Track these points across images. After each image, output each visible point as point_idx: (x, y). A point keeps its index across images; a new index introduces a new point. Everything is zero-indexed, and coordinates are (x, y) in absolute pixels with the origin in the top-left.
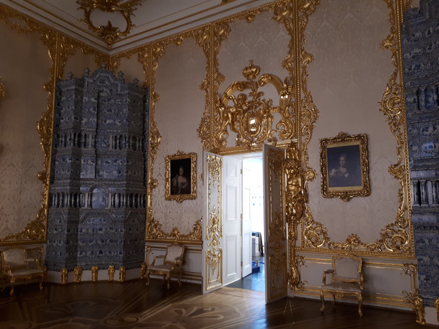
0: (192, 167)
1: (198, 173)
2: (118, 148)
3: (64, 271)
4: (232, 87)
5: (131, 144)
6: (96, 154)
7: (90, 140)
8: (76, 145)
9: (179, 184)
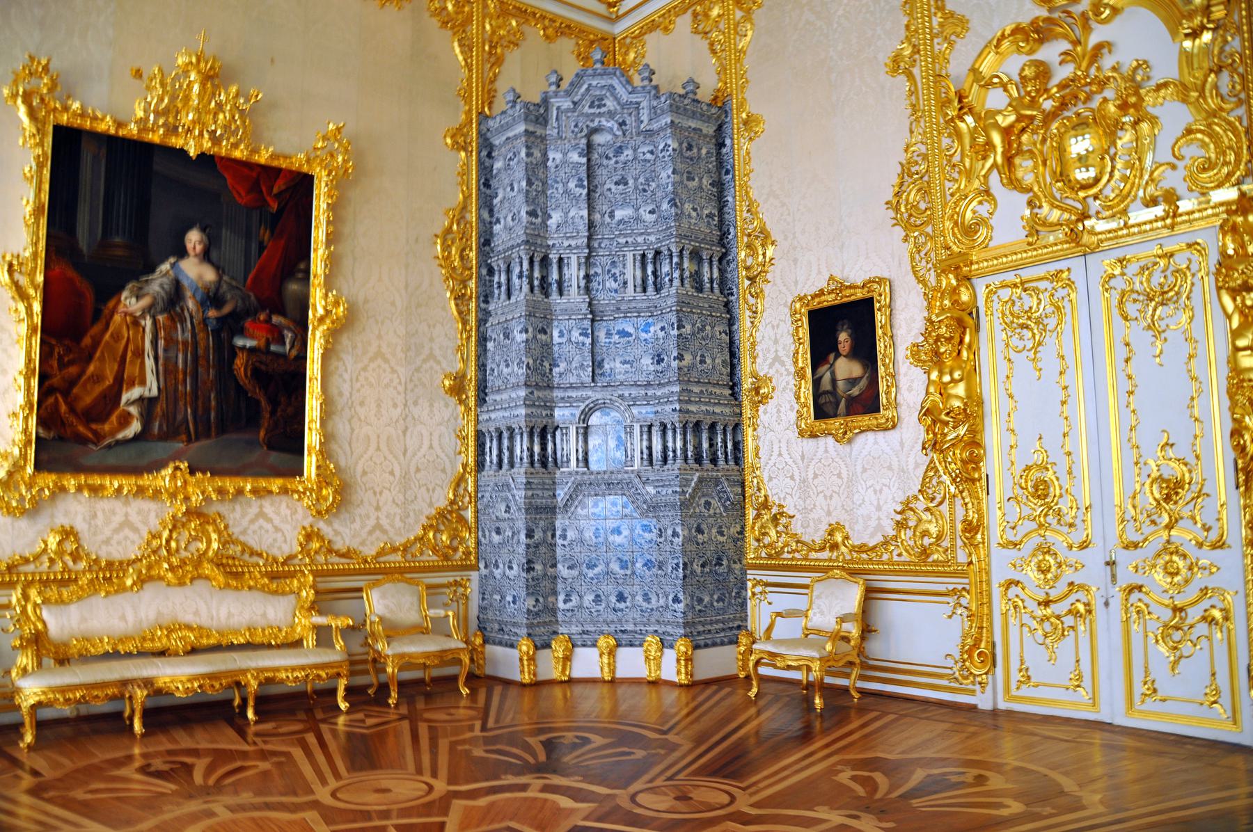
0: (878, 325)
1: (898, 341)
2: (650, 289)
3: (524, 648)
4: (997, 47)
5: (687, 274)
6: (591, 312)
7: (574, 273)
8: (537, 290)
9: (840, 384)
